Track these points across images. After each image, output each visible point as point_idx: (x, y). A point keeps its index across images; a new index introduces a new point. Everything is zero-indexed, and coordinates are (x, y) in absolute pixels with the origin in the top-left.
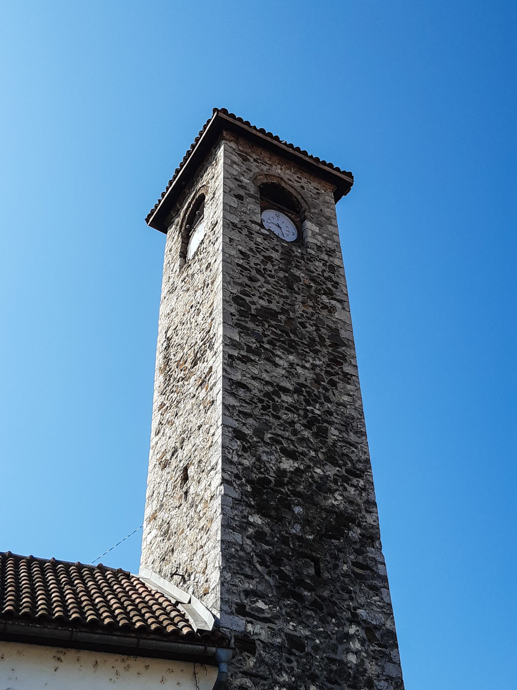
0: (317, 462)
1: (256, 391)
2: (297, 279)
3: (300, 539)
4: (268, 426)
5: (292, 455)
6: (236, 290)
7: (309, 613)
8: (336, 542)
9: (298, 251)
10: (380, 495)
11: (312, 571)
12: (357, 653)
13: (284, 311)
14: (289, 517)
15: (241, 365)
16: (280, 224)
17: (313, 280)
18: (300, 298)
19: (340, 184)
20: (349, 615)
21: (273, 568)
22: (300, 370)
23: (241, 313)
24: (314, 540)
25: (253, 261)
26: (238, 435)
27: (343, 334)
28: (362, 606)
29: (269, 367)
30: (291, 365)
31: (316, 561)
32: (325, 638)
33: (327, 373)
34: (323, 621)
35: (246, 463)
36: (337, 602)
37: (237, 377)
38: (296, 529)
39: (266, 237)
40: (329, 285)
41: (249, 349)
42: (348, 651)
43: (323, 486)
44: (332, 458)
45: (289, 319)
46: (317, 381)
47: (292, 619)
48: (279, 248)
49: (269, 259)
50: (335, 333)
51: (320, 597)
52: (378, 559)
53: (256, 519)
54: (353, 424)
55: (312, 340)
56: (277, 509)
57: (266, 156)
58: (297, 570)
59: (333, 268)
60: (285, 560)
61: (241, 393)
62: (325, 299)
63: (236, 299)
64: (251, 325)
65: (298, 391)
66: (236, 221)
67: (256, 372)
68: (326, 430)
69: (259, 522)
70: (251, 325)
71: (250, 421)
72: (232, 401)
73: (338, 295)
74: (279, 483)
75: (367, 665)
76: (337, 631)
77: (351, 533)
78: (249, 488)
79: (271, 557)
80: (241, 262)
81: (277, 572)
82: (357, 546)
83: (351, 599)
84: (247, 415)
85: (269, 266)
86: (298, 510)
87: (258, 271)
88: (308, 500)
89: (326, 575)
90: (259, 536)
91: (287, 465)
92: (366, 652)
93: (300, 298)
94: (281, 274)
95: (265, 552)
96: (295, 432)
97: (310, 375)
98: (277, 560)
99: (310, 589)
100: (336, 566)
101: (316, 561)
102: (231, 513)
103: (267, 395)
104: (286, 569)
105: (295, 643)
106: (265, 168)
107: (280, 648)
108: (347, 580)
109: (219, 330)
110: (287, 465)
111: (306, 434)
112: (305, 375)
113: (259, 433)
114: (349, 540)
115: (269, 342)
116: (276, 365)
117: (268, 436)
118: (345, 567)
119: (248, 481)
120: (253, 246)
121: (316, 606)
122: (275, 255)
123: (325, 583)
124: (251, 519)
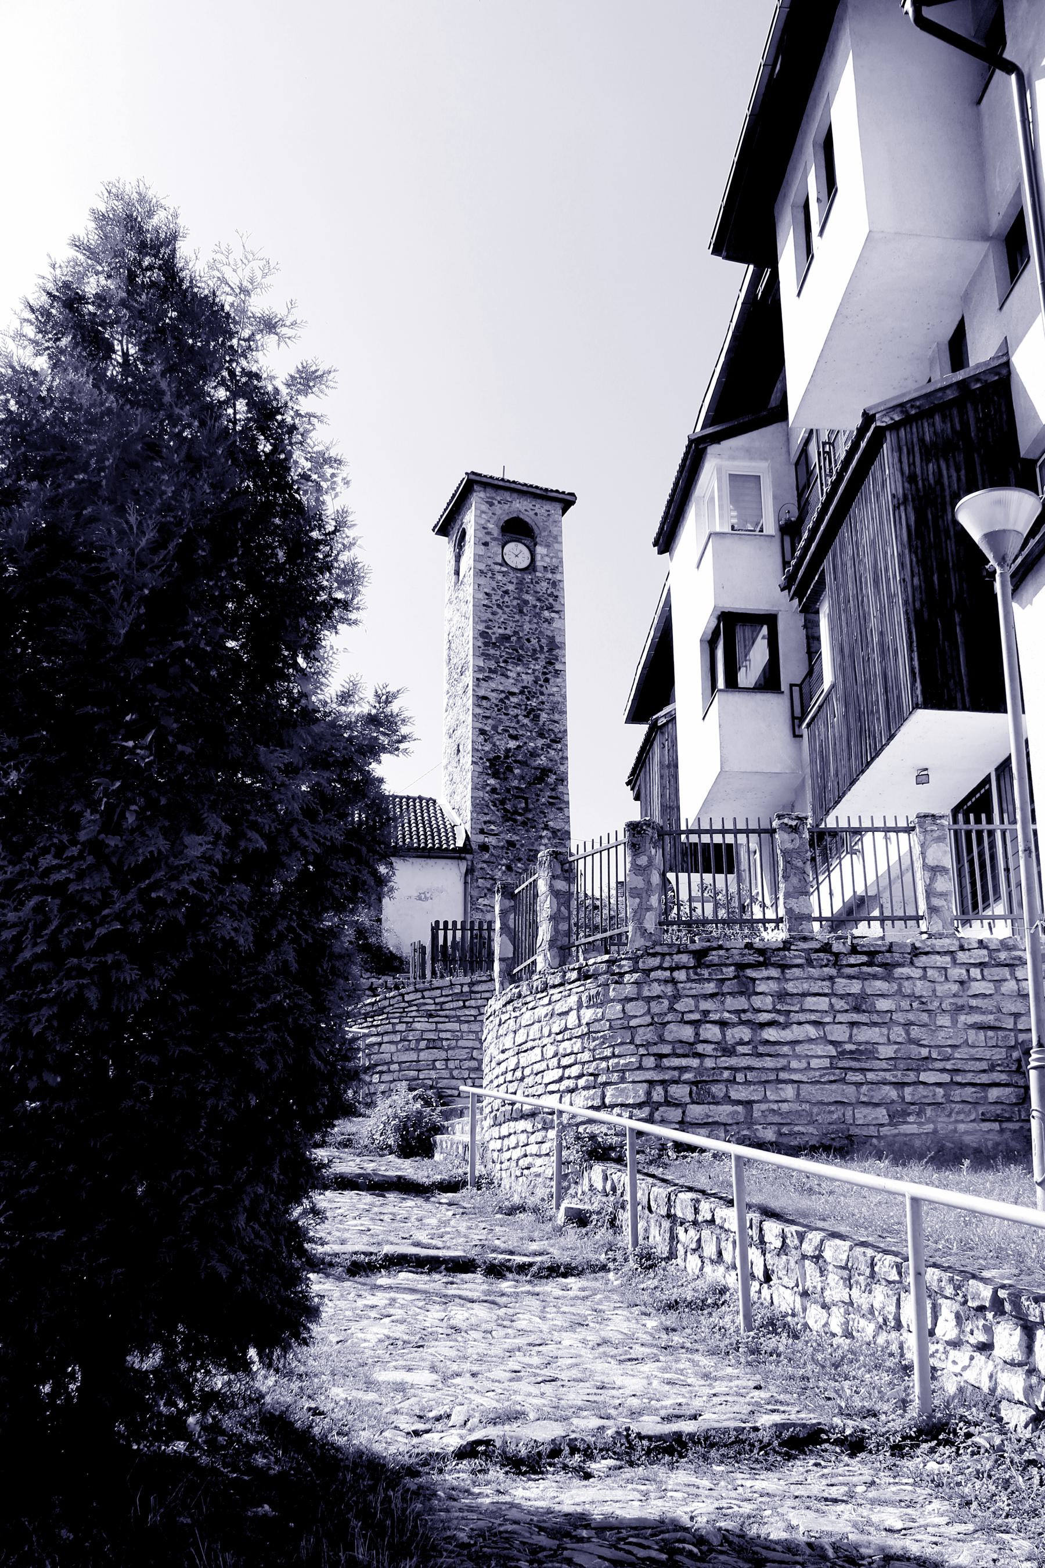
0: (531, 738)
1: (494, 700)
2: (526, 602)
3: (517, 788)
4: (501, 721)
5: (514, 738)
6: (481, 627)
9: (528, 578)
10: (571, 753)
13: (516, 633)
14: (511, 776)
15: (484, 684)
16: (517, 554)
17: (539, 600)
18: (527, 618)
19: (566, 502)
22: (524, 676)
23: (486, 644)
25: (494, 598)
26: (482, 732)
27: (558, 639)
29: (503, 679)
30: (518, 674)
31: (526, 799)
33: (544, 673)
34: (527, 831)
35: (486, 749)
37: (482, 693)
38: (515, 783)
39: (504, 574)
40: (551, 600)
41: (491, 671)
43: (534, 754)
44: (541, 735)
45: (519, 638)
46: (536, 682)
48: (515, 581)
49: (506, 592)
50: (552, 640)
53: (492, 781)
54: (558, 708)
55: (535, 650)
57: (507, 495)
58: (514, 806)
59: (554, 584)
61: (484, 703)
62: (546, 614)
63: (483, 634)
64: (492, 652)
65: (522, 692)
66: (482, 567)
67: (493, 685)
68: (538, 716)
70: (492, 652)
71: (490, 721)
72: (478, 711)
73: (557, 607)
74: (507, 757)
80: (486, 602)
84: (487, 718)
85: (506, 599)
86: (517, 771)
87: (498, 606)
88: (523, 764)
89: (531, 806)
90: (494, 791)
91: (512, 744)
93: (527, 618)
94: (515, 603)
96: (518, 722)
97: (531, 678)
98: (503, 802)
99: (520, 815)
103: (501, 700)
104: (508, 806)
105: (511, 844)
106: (506, 507)
107: (502, 847)
109: (470, 658)
110: (512, 744)
111: (526, 721)
112: (528, 679)
113: (495, 728)
114: (547, 784)
115: (505, 661)
116: (508, 677)
117: (500, 728)
120: (494, 584)
121: (524, 824)
122: (511, 587)
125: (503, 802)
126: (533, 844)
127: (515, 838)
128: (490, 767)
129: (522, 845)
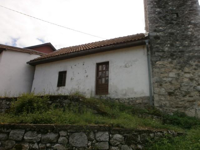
7: (175, 26)
8: (183, 7)
11: (176, 16)
12: (191, 31)
20: (188, 23)
21: (164, 19)
24: (176, 9)
28: (192, 20)
31: (177, 14)
32: (181, 30)
34: (180, 27)
36: (184, 21)
38: (171, 8)
42: (188, 31)
47: (170, 29)
51: (178, 21)
52: (198, 6)
53: (158, 10)
56: (164, 5)
60: (167, 16)
69: (159, 10)
75: (195, 33)
76: (184, 28)
77: (188, 3)
78: (155, 3)
79: (163, 17)
81: (165, 20)
82: (190, 6)
83: (189, 19)
86: (170, 3)
89: (180, 16)
90: (160, 13)
92: (194, 30)
95: (161, 16)
99: (175, 20)
100: (183, 13)
101: (177, 14)
102: (150, 10)
104: (168, 18)
108: (187, 15)
118: (186, 12)
119: (155, 2)
121: (177, 24)
123: (180, 18)
124: (157, 10)
125: (164, 17)
126: (184, 32)
127: (173, 31)
128: (157, 5)
129: (178, 34)
